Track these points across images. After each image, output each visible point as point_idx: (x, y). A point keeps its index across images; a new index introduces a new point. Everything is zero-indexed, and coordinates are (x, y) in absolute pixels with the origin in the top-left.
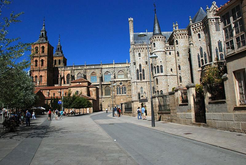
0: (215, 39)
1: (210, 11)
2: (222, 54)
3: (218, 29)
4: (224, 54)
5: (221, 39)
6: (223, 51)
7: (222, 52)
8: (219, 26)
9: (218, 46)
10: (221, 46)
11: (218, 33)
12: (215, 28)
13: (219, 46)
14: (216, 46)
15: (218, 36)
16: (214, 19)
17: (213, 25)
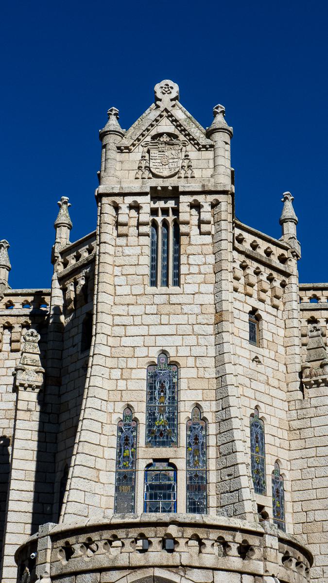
0: (126, 341)
1: (126, 142)
2: (166, 460)
4: (181, 464)
5: (178, 340)
7: (176, 444)
8: (177, 242)
9: (144, 396)
10: (174, 400)
11: (158, 300)
12: (146, 260)
13: (151, 398)
14: (127, 397)
15: (155, 319)
16: (140, 200)
17: (133, 240)
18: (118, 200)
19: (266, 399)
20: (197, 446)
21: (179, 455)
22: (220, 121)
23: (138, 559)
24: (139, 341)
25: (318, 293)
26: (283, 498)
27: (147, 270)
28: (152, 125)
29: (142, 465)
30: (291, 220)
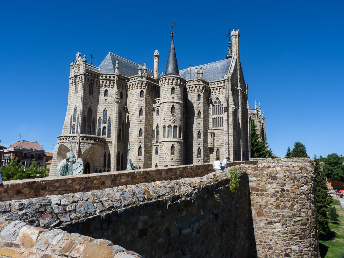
2: (74, 124)
3: (76, 92)
6: (76, 120)
12: (74, 89)
15: (74, 100)
18: (71, 79)
19: (108, 106)
20: (78, 122)
21: (76, 123)
22: (84, 58)
23: (60, 141)
24: (73, 104)
25: (133, 79)
26: (111, 124)
27: (74, 91)
28: (76, 63)
29: (72, 125)
30: (116, 68)
